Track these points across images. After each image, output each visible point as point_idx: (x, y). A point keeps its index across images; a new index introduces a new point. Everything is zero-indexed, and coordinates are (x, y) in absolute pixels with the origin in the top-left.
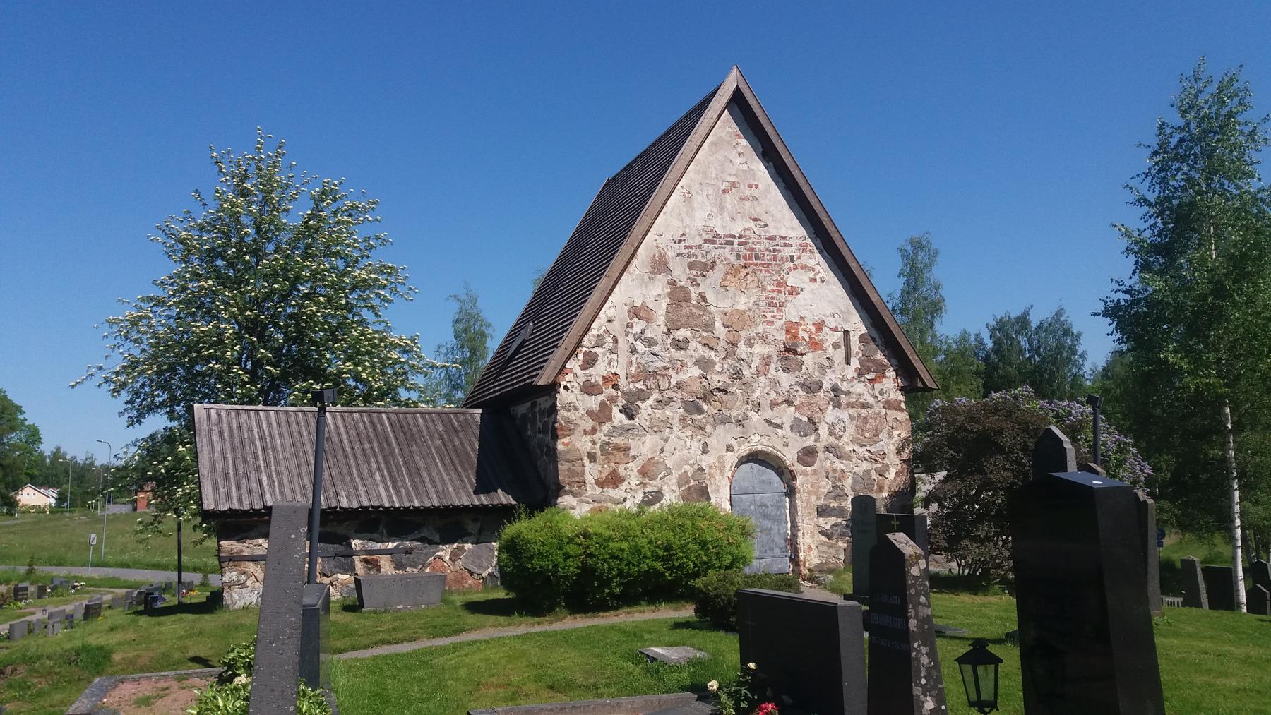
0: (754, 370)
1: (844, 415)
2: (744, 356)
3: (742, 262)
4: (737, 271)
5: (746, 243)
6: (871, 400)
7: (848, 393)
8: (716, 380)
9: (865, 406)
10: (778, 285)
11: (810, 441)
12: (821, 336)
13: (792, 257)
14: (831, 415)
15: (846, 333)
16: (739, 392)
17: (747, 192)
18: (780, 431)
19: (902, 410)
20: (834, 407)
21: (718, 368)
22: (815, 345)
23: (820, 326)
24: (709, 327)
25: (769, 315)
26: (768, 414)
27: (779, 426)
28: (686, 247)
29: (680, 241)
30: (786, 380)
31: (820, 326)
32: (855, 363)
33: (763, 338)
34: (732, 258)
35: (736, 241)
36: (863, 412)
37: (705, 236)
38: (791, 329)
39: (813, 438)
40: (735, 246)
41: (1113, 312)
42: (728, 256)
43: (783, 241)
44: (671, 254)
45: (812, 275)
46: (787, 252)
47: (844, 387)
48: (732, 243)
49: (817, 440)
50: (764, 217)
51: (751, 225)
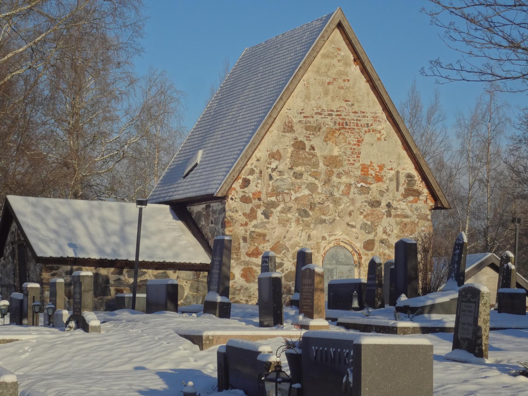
0: (340, 192)
1: (392, 220)
2: (335, 184)
3: (337, 127)
4: (334, 132)
5: (340, 115)
6: (409, 213)
7: (396, 209)
8: (317, 198)
9: (406, 217)
10: (358, 141)
11: (371, 237)
12: (383, 173)
13: (368, 124)
14: (385, 221)
15: (398, 172)
16: (331, 205)
17: (343, 84)
18: (354, 230)
19: (428, 220)
20: (387, 216)
21: (319, 190)
22: (379, 179)
23: (381, 167)
24: (316, 165)
25: (351, 159)
26: (348, 219)
27: (353, 226)
28: (305, 117)
29: (301, 113)
30: (360, 199)
31: (381, 167)
32: (402, 189)
33: (347, 173)
34: (332, 124)
35: (334, 113)
36: (405, 220)
37: (316, 111)
38: (364, 168)
39: (374, 233)
40: (334, 117)
41: (311, 254)
42: (329, 123)
43: (363, 114)
44: (295, 120)
45: (378, 135)
46: (364, 121)
47: (394, 204)
48: (331, 115)
49: (375, 236)
50: (351, 100)
51: (344, 104)
